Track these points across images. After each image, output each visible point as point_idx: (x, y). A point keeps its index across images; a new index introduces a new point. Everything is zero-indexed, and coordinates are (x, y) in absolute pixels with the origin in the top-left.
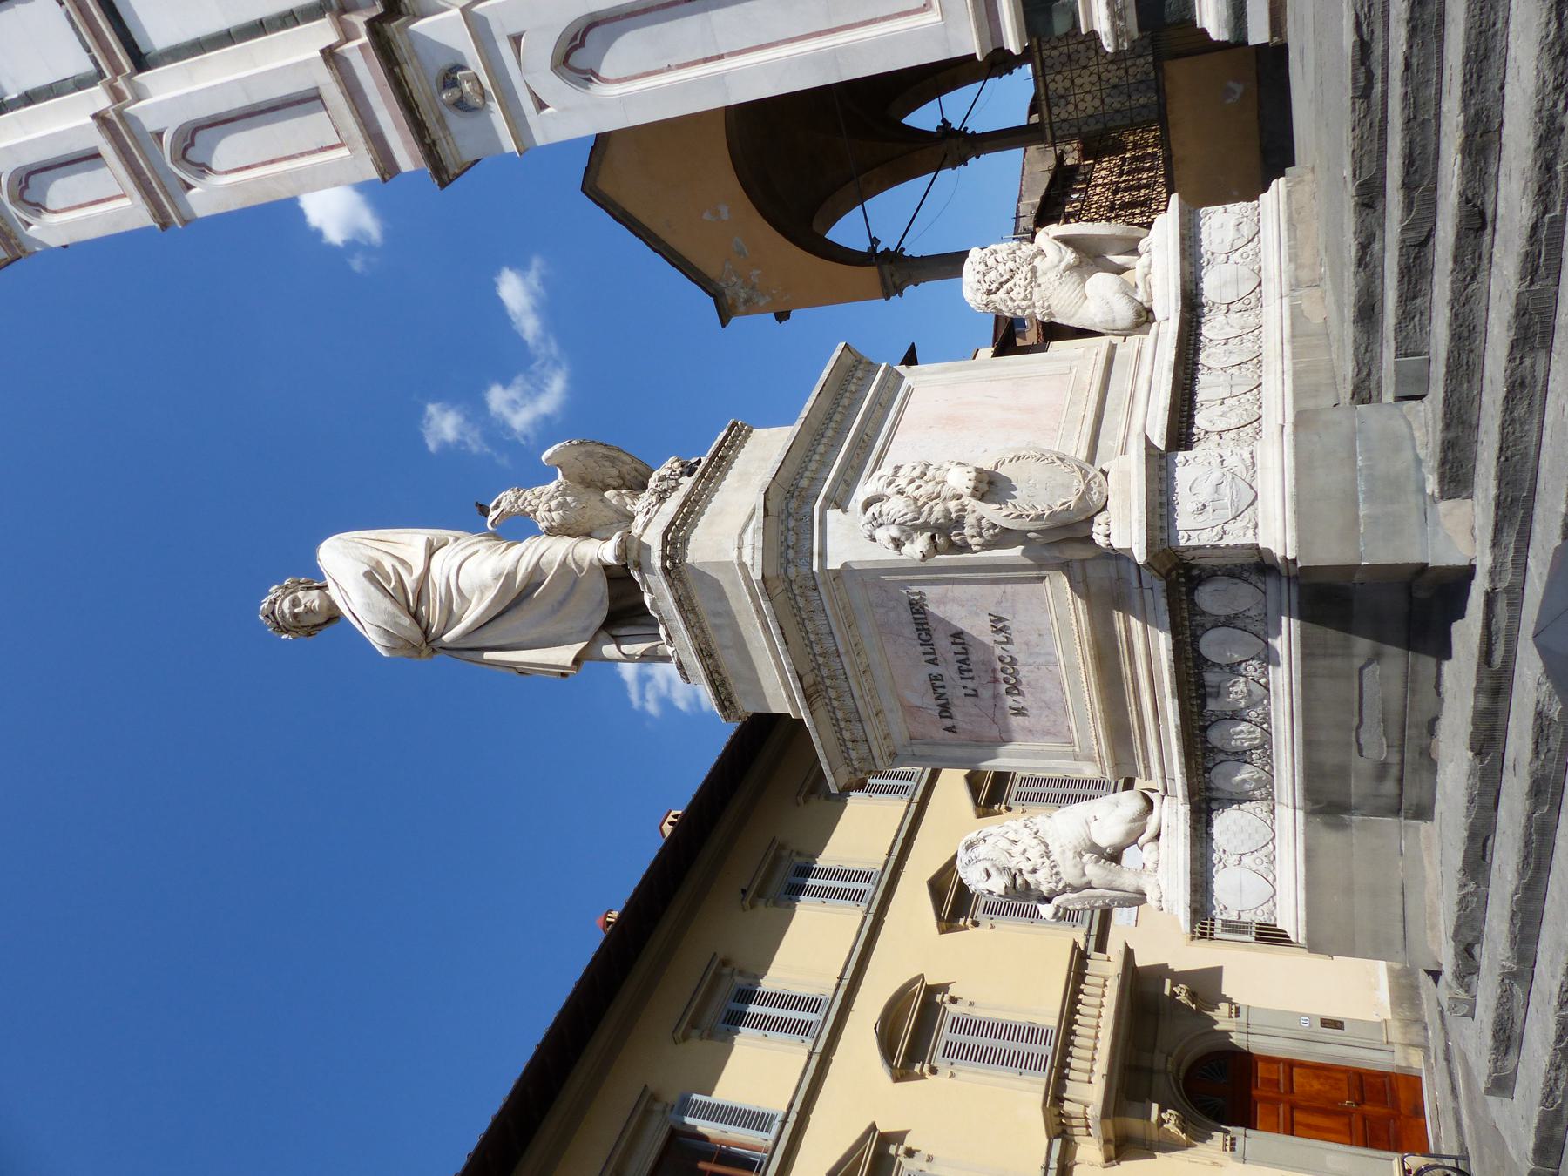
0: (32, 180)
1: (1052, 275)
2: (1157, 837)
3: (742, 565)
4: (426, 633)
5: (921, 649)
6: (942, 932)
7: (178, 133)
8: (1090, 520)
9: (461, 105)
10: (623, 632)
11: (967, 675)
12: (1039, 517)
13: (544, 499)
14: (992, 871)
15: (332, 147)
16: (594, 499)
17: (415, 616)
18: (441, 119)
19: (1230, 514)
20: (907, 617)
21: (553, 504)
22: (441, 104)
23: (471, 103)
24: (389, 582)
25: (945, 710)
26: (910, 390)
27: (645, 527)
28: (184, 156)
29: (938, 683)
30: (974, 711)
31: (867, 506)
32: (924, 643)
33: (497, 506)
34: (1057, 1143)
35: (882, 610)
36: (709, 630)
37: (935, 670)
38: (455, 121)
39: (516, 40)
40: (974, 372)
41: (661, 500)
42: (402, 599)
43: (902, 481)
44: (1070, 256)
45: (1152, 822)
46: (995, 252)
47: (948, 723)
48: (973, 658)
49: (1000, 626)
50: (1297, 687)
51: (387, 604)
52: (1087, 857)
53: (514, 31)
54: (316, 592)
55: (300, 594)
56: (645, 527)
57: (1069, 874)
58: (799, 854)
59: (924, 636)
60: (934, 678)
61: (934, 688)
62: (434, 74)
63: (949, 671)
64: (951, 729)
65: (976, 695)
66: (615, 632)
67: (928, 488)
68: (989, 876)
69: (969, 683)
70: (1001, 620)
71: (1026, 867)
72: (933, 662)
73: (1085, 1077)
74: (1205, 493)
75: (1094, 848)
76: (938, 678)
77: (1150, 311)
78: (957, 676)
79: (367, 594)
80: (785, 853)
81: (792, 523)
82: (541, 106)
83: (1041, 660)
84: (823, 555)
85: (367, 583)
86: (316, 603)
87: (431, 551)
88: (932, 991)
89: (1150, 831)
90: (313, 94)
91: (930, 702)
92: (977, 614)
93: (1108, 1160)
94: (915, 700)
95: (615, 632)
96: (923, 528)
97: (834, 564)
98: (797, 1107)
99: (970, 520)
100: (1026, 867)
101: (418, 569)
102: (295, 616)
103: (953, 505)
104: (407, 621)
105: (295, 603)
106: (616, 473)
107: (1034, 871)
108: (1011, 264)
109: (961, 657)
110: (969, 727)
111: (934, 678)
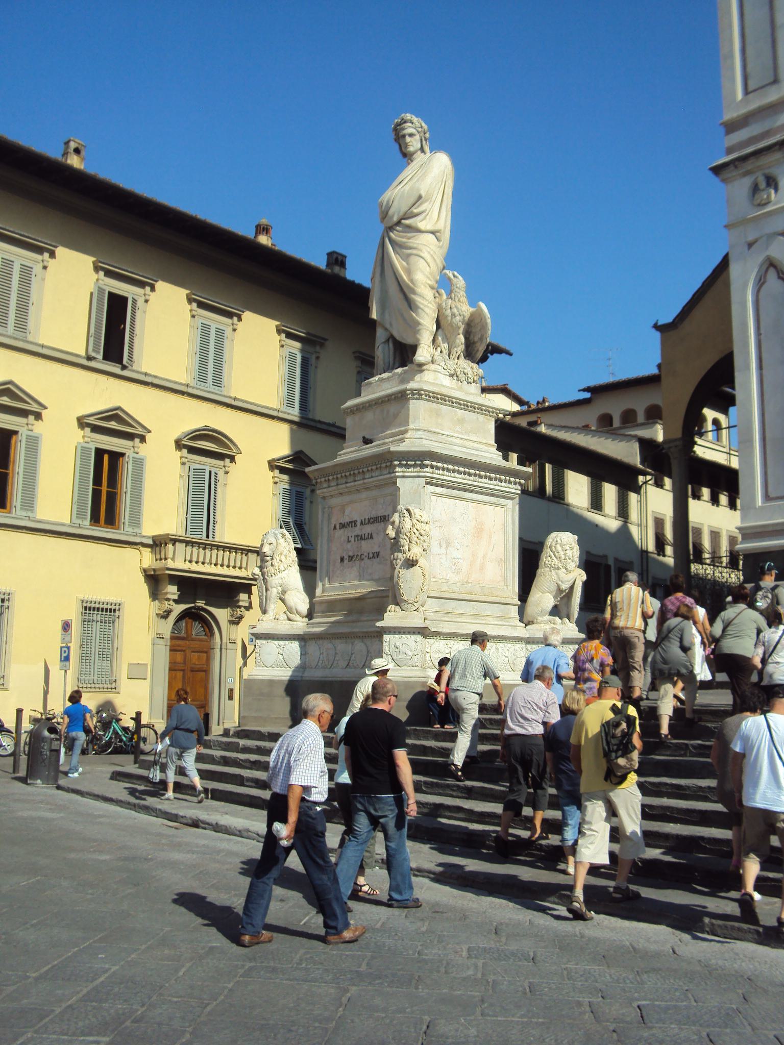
1: (555, 577)
3: (406, 431)
6: (269, 462)
8: (397, 604)
9: (755, 189)
10: (391, 345)
12: (398, 583)
16: (461, 331)
17: (399, 223)
19: (395, 657)
21: (455, 310)
23: (757, 196)
25: (343, 526)
26: (502, 506)
27: (435, 371)
31: (408, 511)
32: (369, 520)
33: (454, 276)
34: (150, 542)
37: (358, 523)
38: (747, 182)
40: (511, 539)
41: (452, 375)
43: (418, 526)
44: (565, 586)
45: (298, 618)
46: (572, 548)
47: (338, 526)
52: (280, 589)
54: (419, 146)
56: (435, 371)
58: (318, 358)
61: (351, 522)
62: (774, 171)
63: (358, 530)
64: (335, 528)
66: (391, 341)
67: (414, 539)
69: (353, 539)
72: (362, 523)
73: (188, 558)
74: (402, 649)
75: (284, 592)
76: (356, 525)
77: (533, 623)
78: (355, 534)
80: (318, 348)
82: (750, 245)
86: (411, 149)
87: (433, 233)
88: (232, 459)
89: (291, 616)
91: (347, 520)
93: (145, 570)
94: (347, 512)
95: (391, 341)
97: (399, 482)
100: (274, 562)
102: (404, 136)
103: (406, 548)
104: (395, 219)
105: (411, 135)
107: (272, 565)
108: (563, 557)
111: (355, 522)
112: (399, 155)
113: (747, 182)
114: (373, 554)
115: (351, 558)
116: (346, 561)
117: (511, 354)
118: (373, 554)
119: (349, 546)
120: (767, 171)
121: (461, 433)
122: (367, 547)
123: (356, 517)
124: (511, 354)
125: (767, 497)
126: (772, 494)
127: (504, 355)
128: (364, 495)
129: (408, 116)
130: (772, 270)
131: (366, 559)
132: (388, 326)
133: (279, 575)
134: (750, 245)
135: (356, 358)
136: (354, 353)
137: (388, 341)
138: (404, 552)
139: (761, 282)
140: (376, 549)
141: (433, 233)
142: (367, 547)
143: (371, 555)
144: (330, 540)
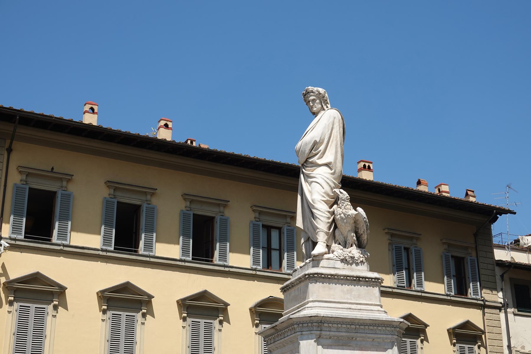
10: (310, 242)
13: (344, 211)
21: (342, 215)
27: (328, 259)
33: (341, 193)
36: (299, 286)
42: (310, 156)
51: (307, 151)
55: (318, 101)
56: (328, 259)
79: (309, 143)
81: (309, 324)
87: (327, 165)
98: (231, 270)
101: (320, 162)
105: (314, 101)
106: (362, 233)
112: (311, 114)
117: (515, 213)
121: (351, 299)
124: (515, 213)
129: (310, 88)
141: (327, 165)
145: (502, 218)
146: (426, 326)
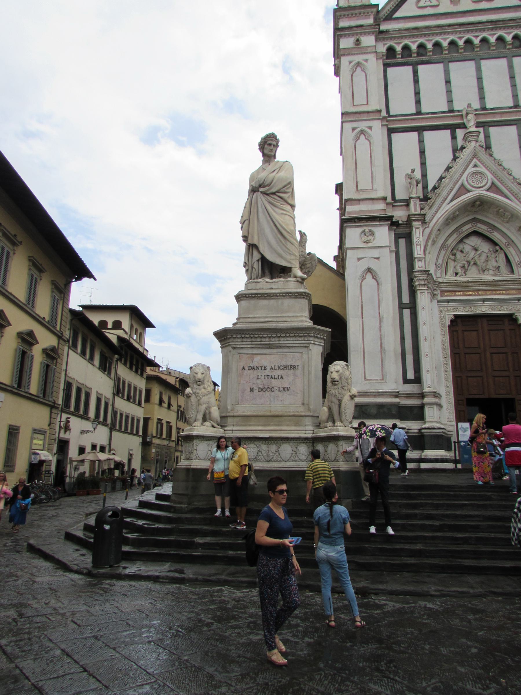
0: (364, 74)
2: (213, 426)
4: (267, 194)
5: (277, 365)
7: (370, 136)
10: (260, 263)
11: (266, 378)
14: (203, 375)
15: (357, 186)
17: (274, 193)
18: (360, 226)
20: (289, 364)
22: (364, 228)
24: (287, 189)
25: (252, 368)
28: (362, 133)
29: (263, 368)
30: (252, 377)
35: (292, 357)
37: (268, 368)
39: (378, 258)
42: (281, 191)
47: (247, 368)
48: (273, 380)
49: (286, 389)
50: (273, 469)
53: (380, 259)
57: (204, 399)
58: (14, 254)
59: (281, 367)
60: (265, 367)
61: (261, 367)
62: (373, 229)
63: (268, 372)
64: (244, 368)
65: (258, 379)
68: (203, 374)
69: (263, 377)
70: (288, 390)
71: (206, 386)
72: (272, 368)
78: (266, 374)
82: (359, 259)
83: (272, 399)
84: (314, 344)
85: (288, 181)
89: (215, 425)
90: (374, 188)
91: (255, 364)
92: (289, 384)
94: (257, 359)
96: (341, 378)
97: (311, 346)
99: (343, 392)
103: (346, 388)
104: (274, 190)
105: (274, 146)
107: (204, 388)
109: (273, 377)
110: (245, 374)
111: (265, 367)
113: (360, 230)
114: (284, 389)
115: (261, 390)
116: (256, 391)
117: (95, 279)
118: (284, 389)
119: (259, 381)
120: (370, 228)
122: (275, 383)
123: (264, 363)
124: (95, 279)
125: (365, 379)
126: (368, 377)
127: (92, 279)
128: (275, 351)
130: (369, 274)
131: (277, 392)
132: (262, 252)
133: (209, 396)
134: (359, 259)
135: (30, 260)
136: (29, 257)
137: (258, 261)
138: (345, 390)
139: (363, 278)
140: (287, 386)
142: (275, 383)
143: (281, 389)
144: (240, 376)
145: (85, 280)
146: (37, 342)
